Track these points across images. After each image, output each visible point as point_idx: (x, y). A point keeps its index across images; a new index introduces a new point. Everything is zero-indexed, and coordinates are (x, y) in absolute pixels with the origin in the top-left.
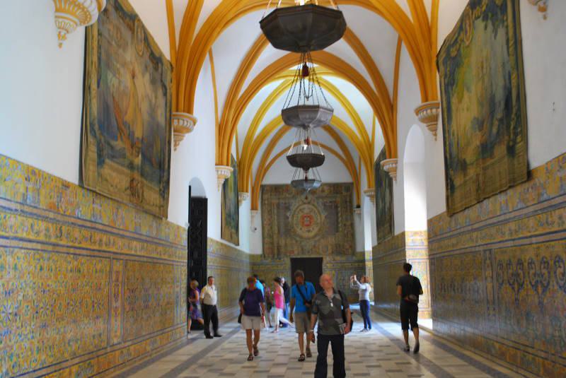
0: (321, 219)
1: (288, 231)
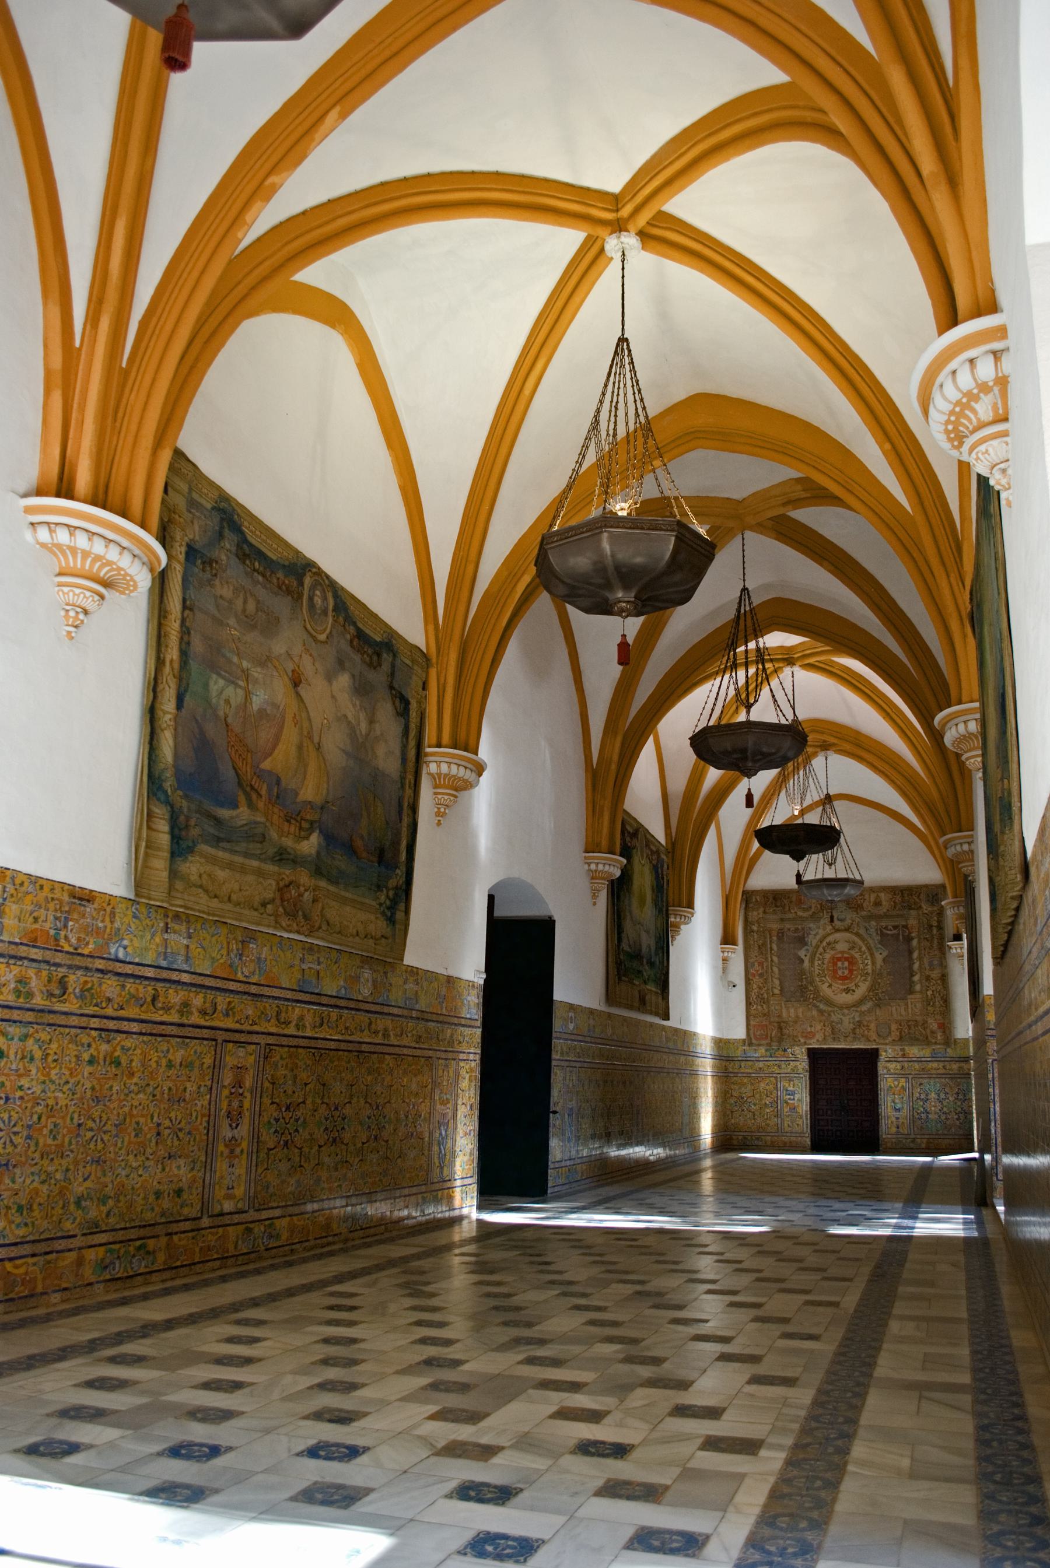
0: (874, 963)
1: (802, 990)
